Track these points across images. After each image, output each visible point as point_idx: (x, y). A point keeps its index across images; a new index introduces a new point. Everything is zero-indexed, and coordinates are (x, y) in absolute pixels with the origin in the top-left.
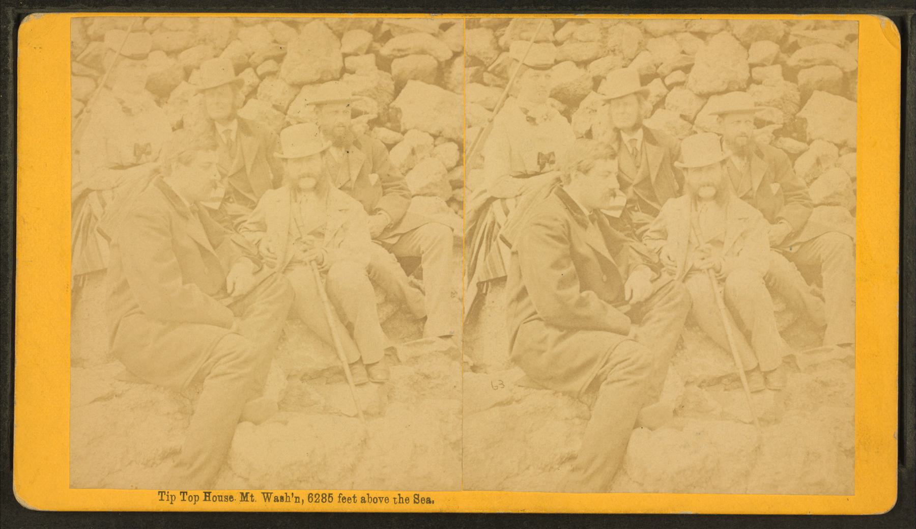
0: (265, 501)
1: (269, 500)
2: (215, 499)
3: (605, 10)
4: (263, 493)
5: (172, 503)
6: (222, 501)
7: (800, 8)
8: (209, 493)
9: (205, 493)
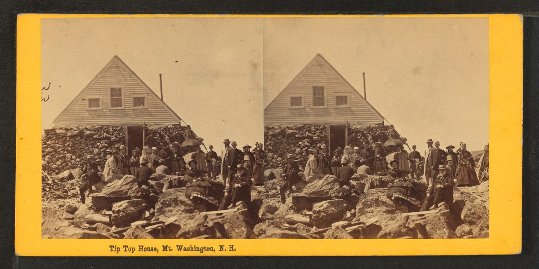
0: (179, 251)
1: (181, 251)
2: (145, 250)
4: (177, 246)
5: (117, 253)
8: (142, 246)
9: (140, 246)
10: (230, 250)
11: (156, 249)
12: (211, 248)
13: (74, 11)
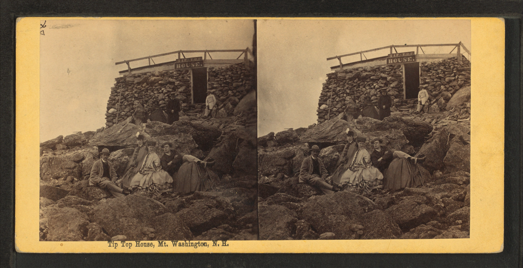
3: (351, 15)
5: (115, 248)
6: (146, 246)
7: (463, 14)
10: (223, 245)
11: (152, 244)
12: (204, 243)
13: (69, 13)
